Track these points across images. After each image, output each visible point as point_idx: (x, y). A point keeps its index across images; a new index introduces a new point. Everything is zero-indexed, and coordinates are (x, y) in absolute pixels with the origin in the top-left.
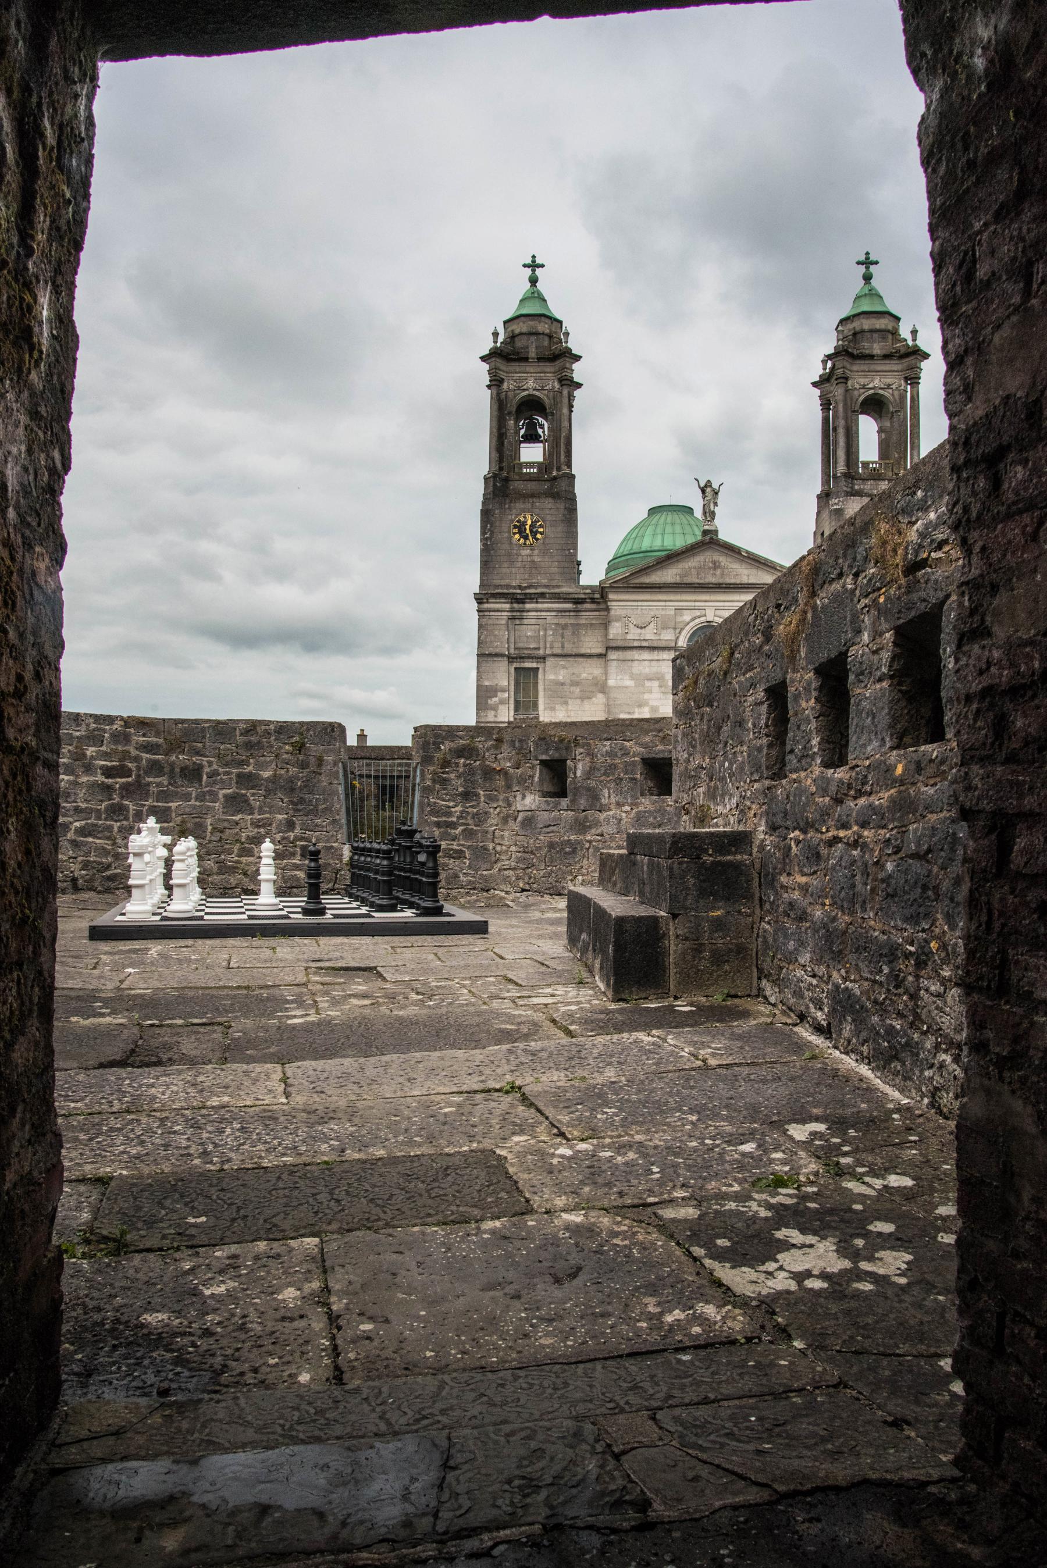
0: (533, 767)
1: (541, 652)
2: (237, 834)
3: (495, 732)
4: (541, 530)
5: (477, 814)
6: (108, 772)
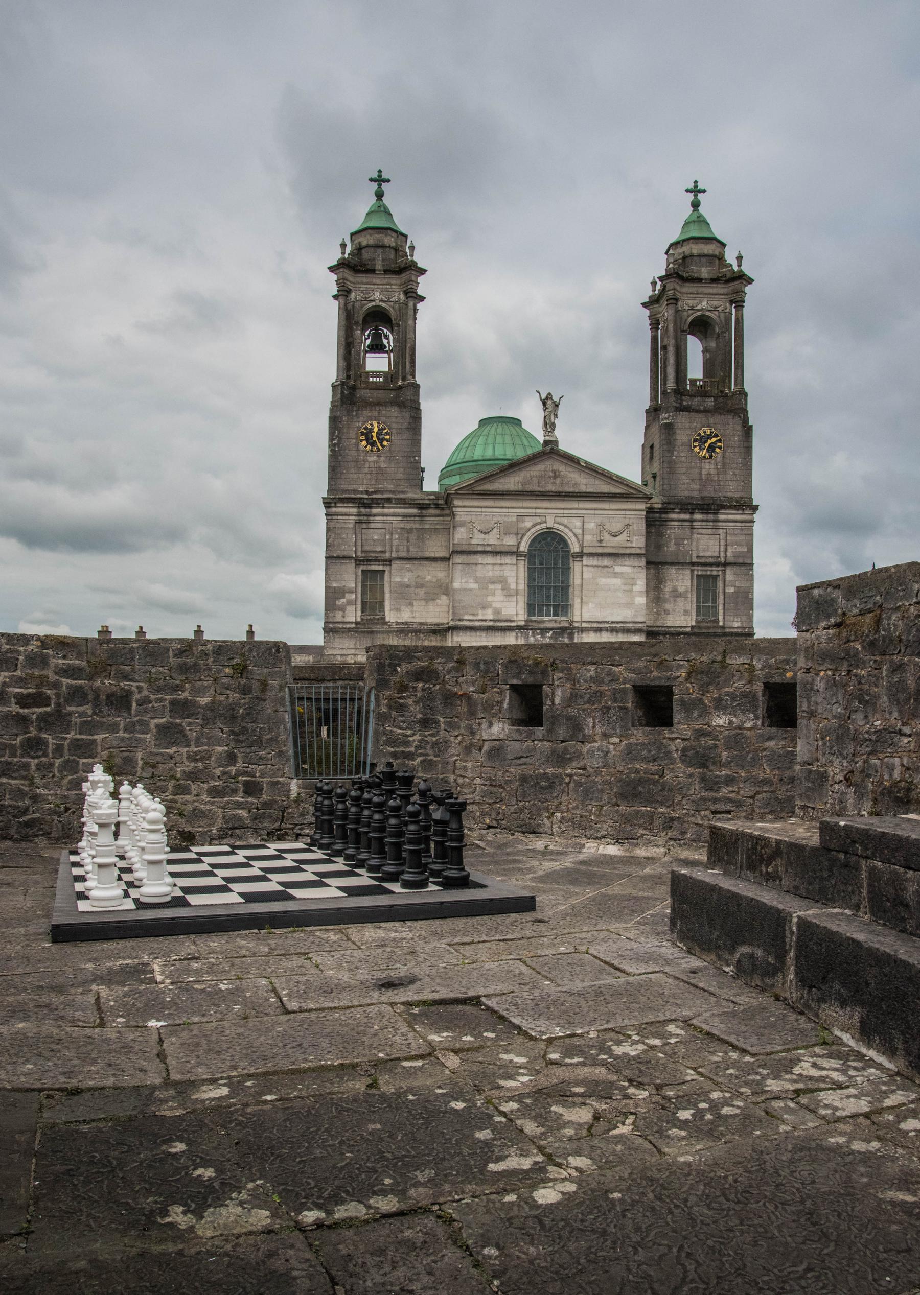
0: (501, 692)
1: (387, 555)
2: (171, 769)
3: (456, 652)
4: (387, 437)
5: (437, 743)
6: (23, 701)
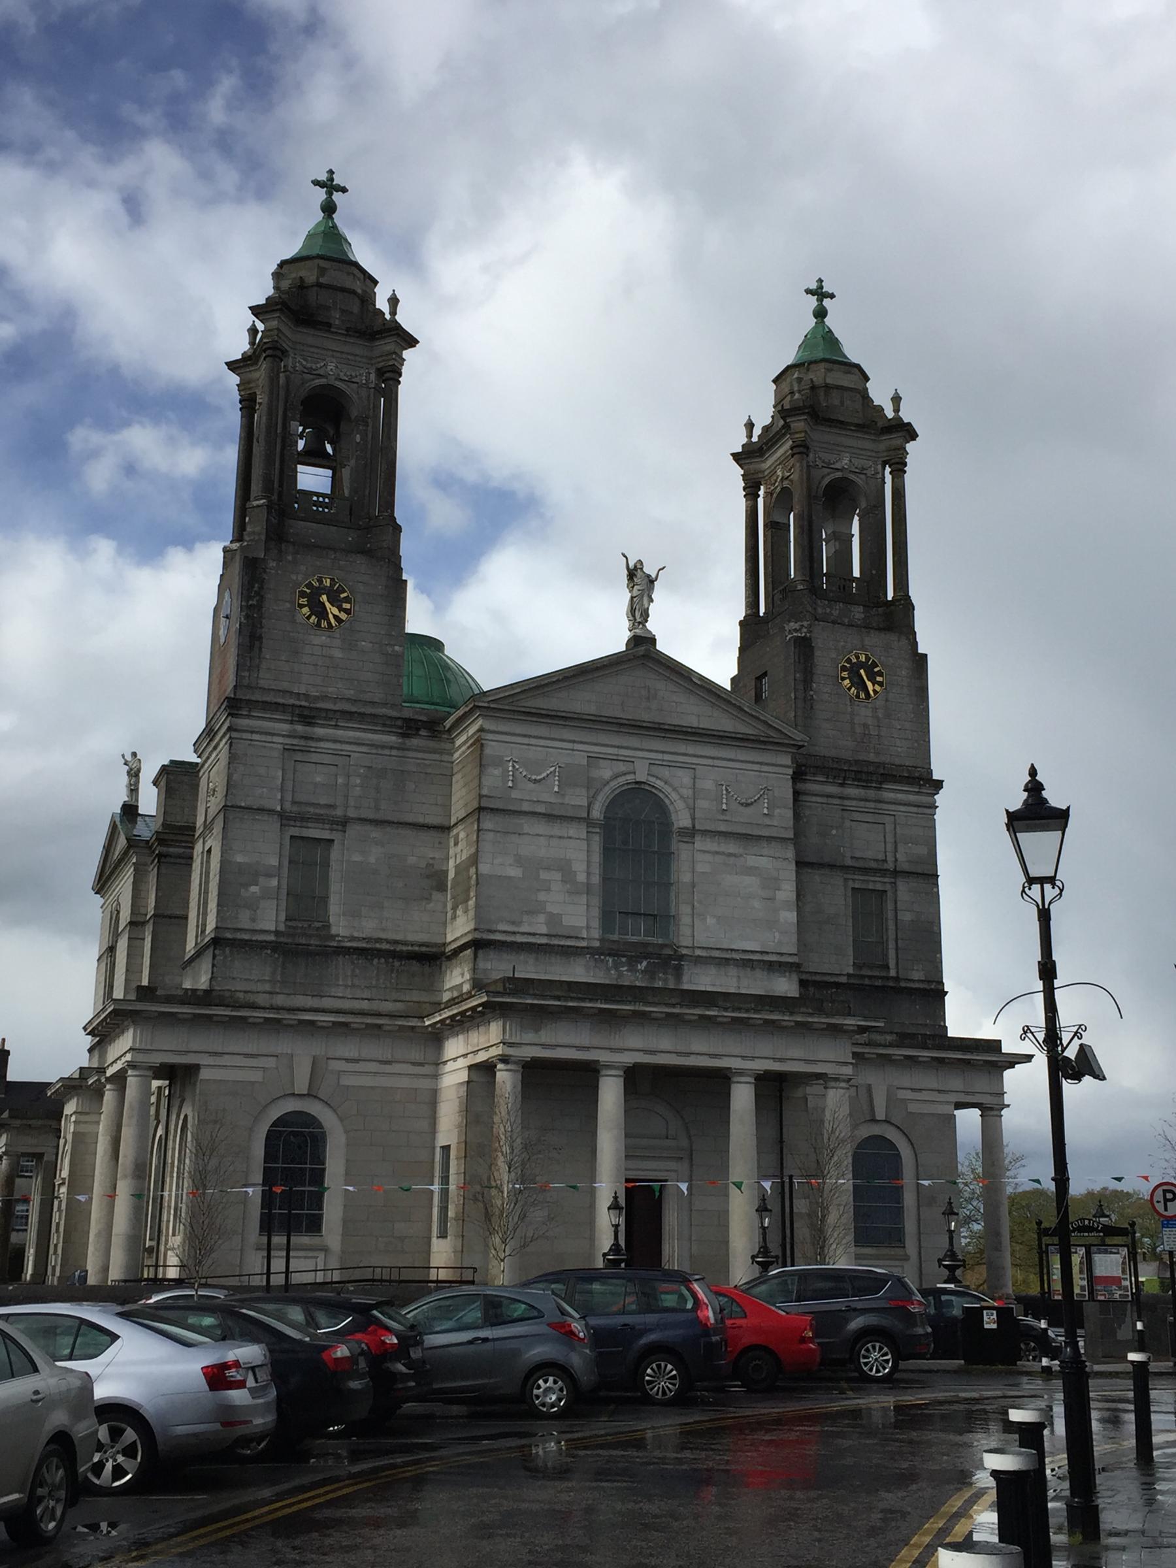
1: (339, 812)
